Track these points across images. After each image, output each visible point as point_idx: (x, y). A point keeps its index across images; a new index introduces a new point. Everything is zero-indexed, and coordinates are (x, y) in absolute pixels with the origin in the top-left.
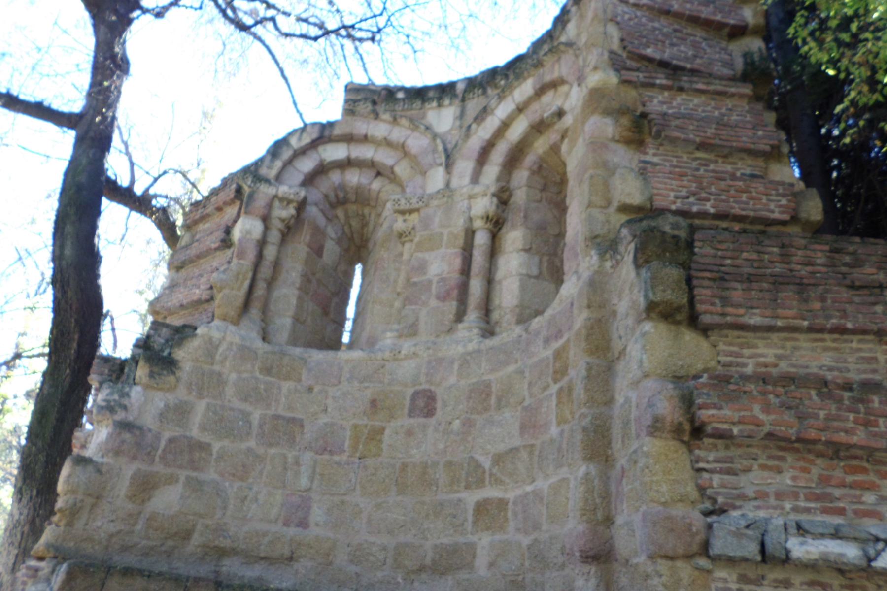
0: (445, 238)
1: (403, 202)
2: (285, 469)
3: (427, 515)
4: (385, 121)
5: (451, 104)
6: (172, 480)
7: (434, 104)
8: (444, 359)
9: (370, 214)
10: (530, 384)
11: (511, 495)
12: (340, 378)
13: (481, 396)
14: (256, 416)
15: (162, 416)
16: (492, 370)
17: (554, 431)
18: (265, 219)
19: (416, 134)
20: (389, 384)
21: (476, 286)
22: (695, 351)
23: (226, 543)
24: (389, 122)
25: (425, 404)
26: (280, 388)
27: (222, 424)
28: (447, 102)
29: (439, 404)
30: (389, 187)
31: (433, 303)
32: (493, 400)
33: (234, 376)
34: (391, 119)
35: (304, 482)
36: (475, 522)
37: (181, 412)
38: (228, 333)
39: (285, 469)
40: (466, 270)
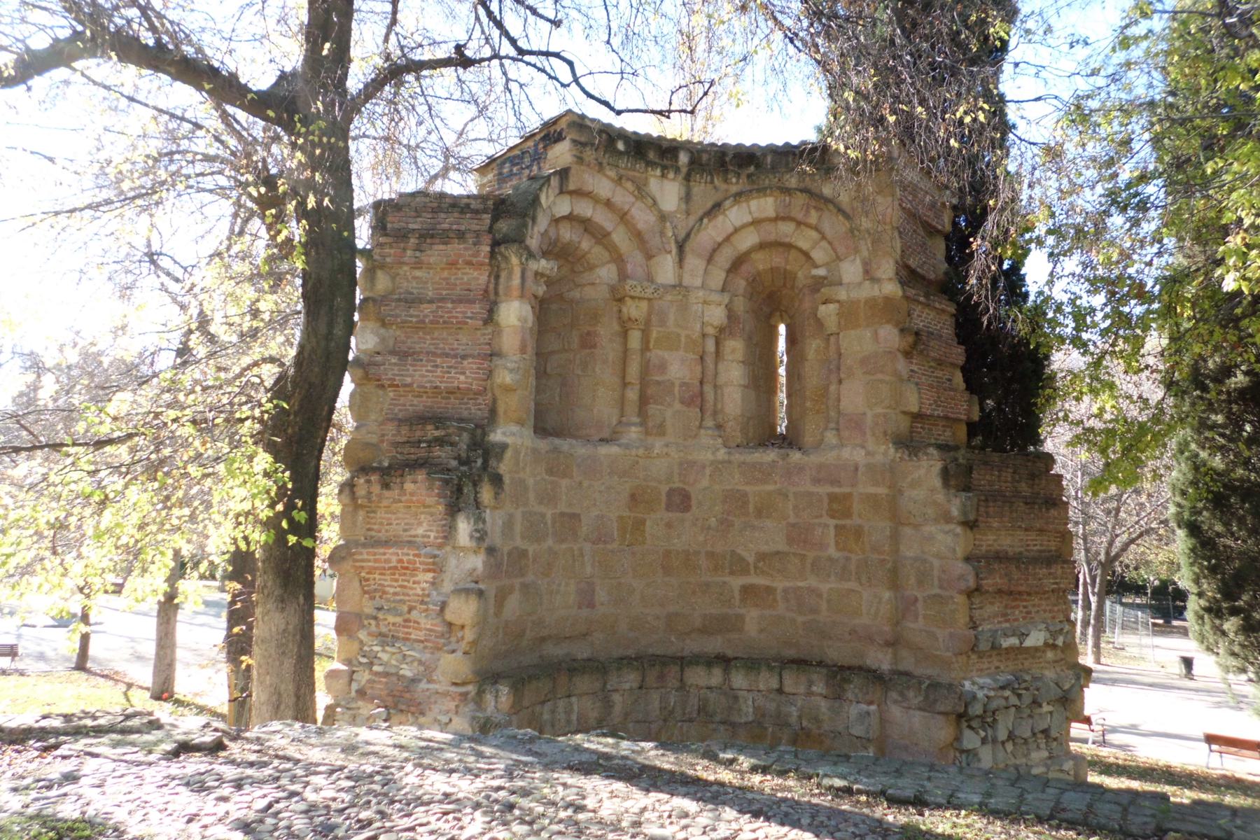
0: (683, 339)
2: (574, 561)
3: (694, 593)
4: (608, 177)
5: (674, 179)
6: (511, 590)
7: (658, 172)
10: (795, 507)
11: (780, 584)
13: (737, 500)
14: (549, 514)
16: (747, 483)
17: (832, 551)
19: (639, 204)
23: (545, 633)
24: (613, 180)
25: (681, 500)
28: (671, 175)
29: (694, 503)
31: (677, 406)
32: (751, 508)
35: (589, 570)
36: (742, 600)
39: (574, 561)
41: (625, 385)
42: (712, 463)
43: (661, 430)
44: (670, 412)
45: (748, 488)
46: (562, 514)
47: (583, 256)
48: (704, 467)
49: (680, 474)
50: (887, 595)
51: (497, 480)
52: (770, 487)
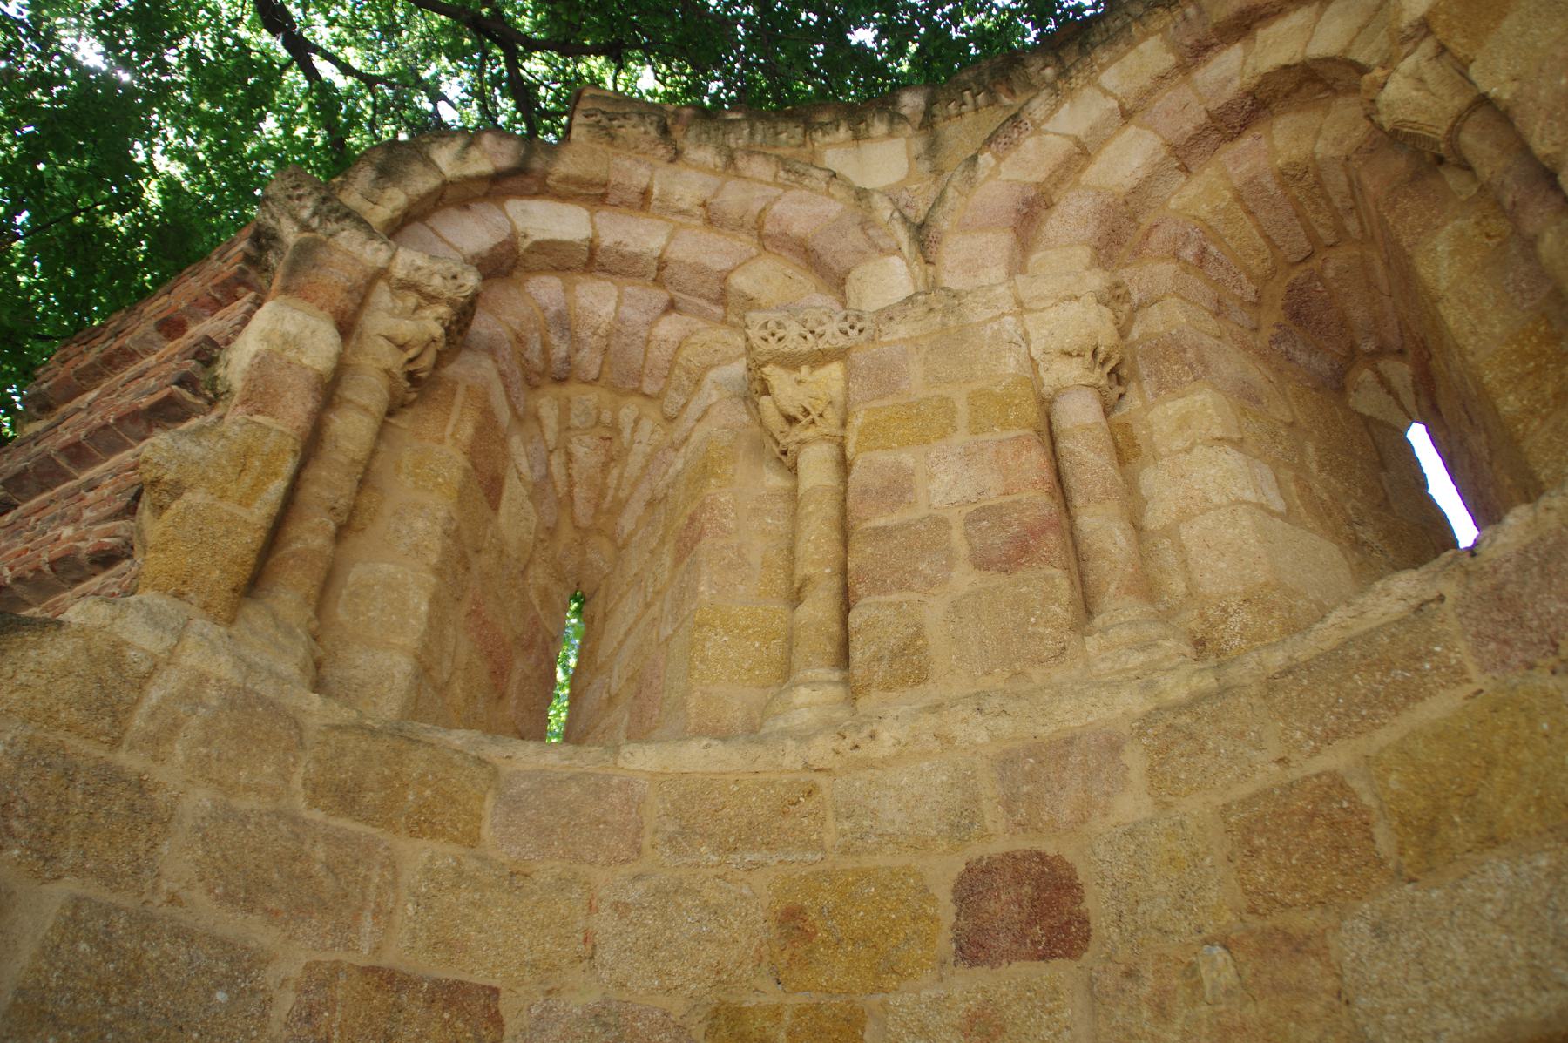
1: (793, 330)
4: (700, 167)
8: (1069, 742)
9: (636, 421)
12: (638, 834)
20: (846, 851)
26: (392, 865)
29: (1097, 903)
31: (964, 578)
33: (201, 799)
34: (720, 162)
38: (191, 641)
41: (796, 597)
42: (1147, 719)
43: (910, 664)
44: (942, 604)
45: (1336, 759)
46: (387, 979)
47: (673, 363)
48: (1114, 747)
49: (1009, 804)
52: (1439, 707)
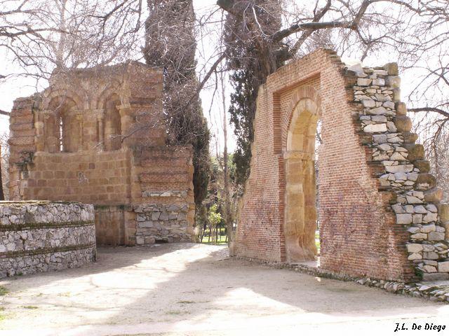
6: (40, 189)
15: (36, 177)
18: (43, 121)
21: (101, 136)
22: (141, 170)
27: (47, 175)
30: (71, 102)
37: (38, 174)
40: (98, 133)
50: (126, 185)
51: (32, 165)
